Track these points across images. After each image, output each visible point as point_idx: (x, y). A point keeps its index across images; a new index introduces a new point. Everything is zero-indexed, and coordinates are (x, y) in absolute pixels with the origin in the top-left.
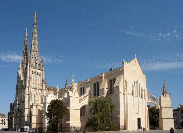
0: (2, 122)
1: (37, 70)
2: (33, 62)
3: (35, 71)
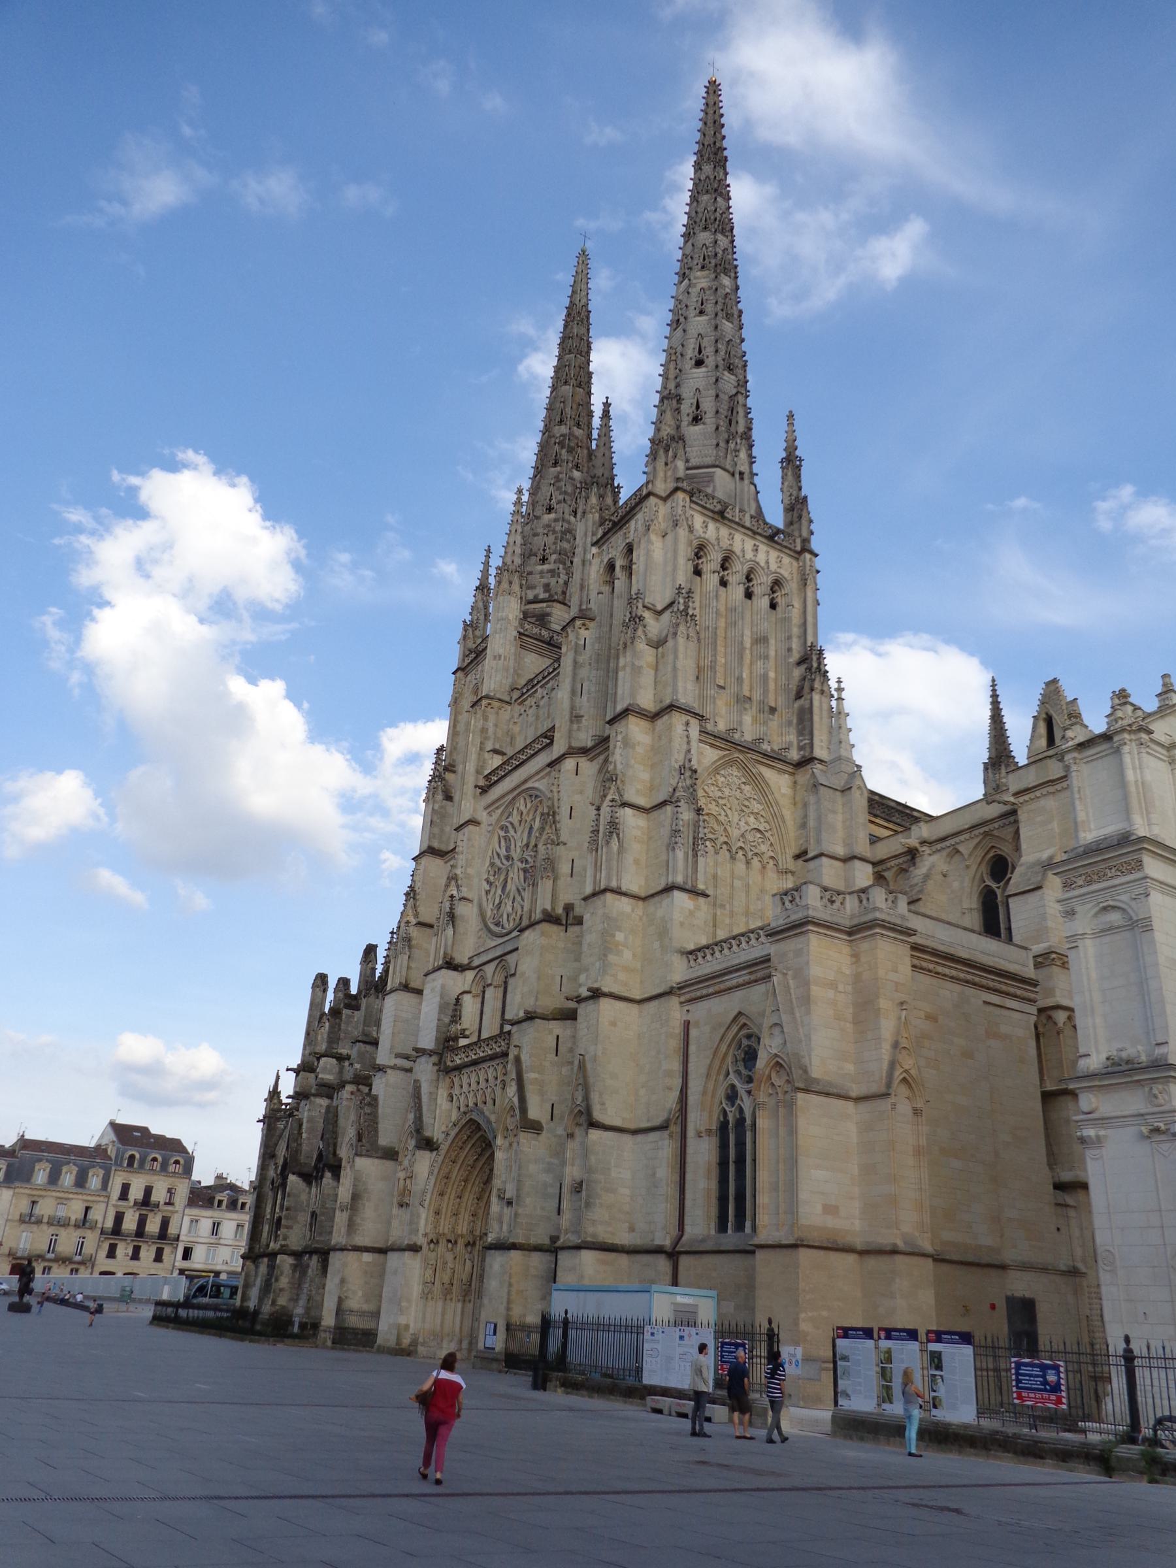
0: (142, 1222)
1: (749, 544)
2: (709, 460)
3: (725, 543)
